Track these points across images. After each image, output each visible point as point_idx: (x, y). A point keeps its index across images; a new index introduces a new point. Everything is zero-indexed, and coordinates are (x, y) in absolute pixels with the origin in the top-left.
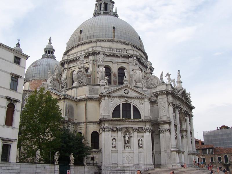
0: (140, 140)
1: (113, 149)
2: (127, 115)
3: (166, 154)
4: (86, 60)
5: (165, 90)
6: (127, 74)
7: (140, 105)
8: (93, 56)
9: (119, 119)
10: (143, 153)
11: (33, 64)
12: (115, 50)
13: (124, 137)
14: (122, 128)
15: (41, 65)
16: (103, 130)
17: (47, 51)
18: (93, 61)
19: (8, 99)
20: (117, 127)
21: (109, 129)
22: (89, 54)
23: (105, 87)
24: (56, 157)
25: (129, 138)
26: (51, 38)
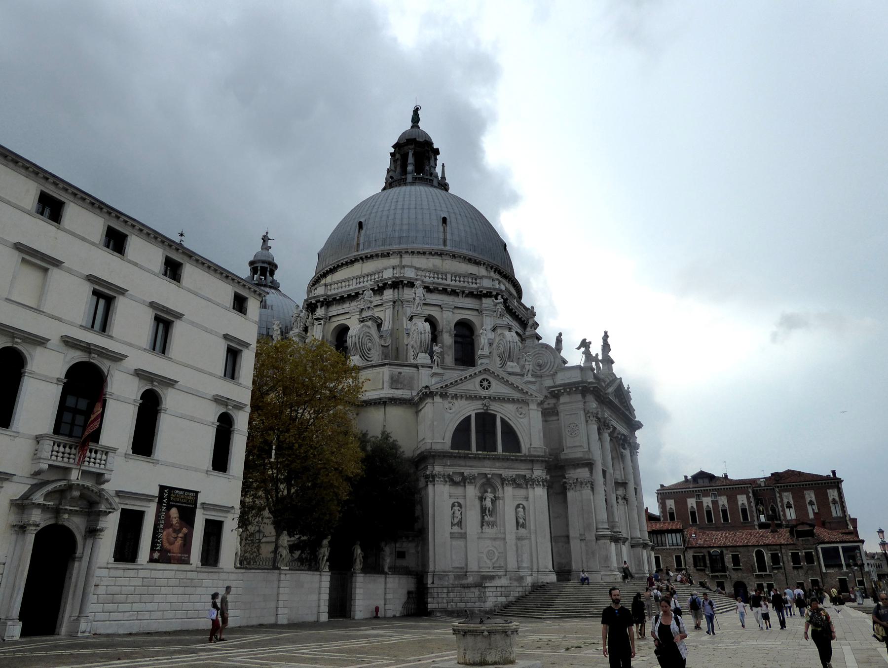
0: (520, 507)
3: (583, 544)
4: (376, 300)
5: (578, 383)
8: (394, 290)
9: (468, 452)
10: (526, 542)
12: (449, 276)
14: (476, 475)
16: (431, 482)
17: (259, 268)
18: (394, 302)
19: (218, 400)
20: (463, 473)
21: (444, 479)
23: (434, 371)
24: (325, 552)
25: (492, 503)
26: (267, 233)
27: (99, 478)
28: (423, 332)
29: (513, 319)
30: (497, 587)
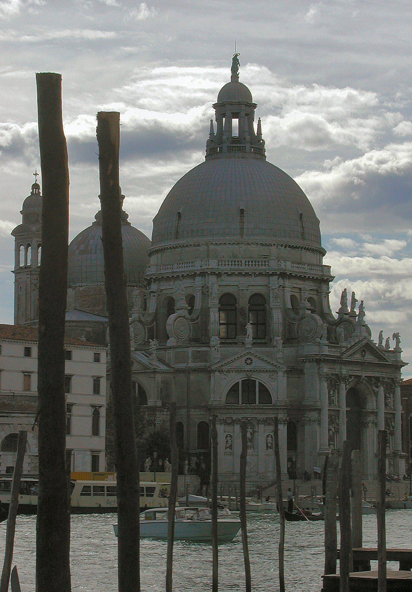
1: (225, 451)
7: (271, 383)
8: (202, 277)
12: (243, 262)
19: (93, 406)
20: (232, 418)
22: (196, 273)
28: (214, 323)
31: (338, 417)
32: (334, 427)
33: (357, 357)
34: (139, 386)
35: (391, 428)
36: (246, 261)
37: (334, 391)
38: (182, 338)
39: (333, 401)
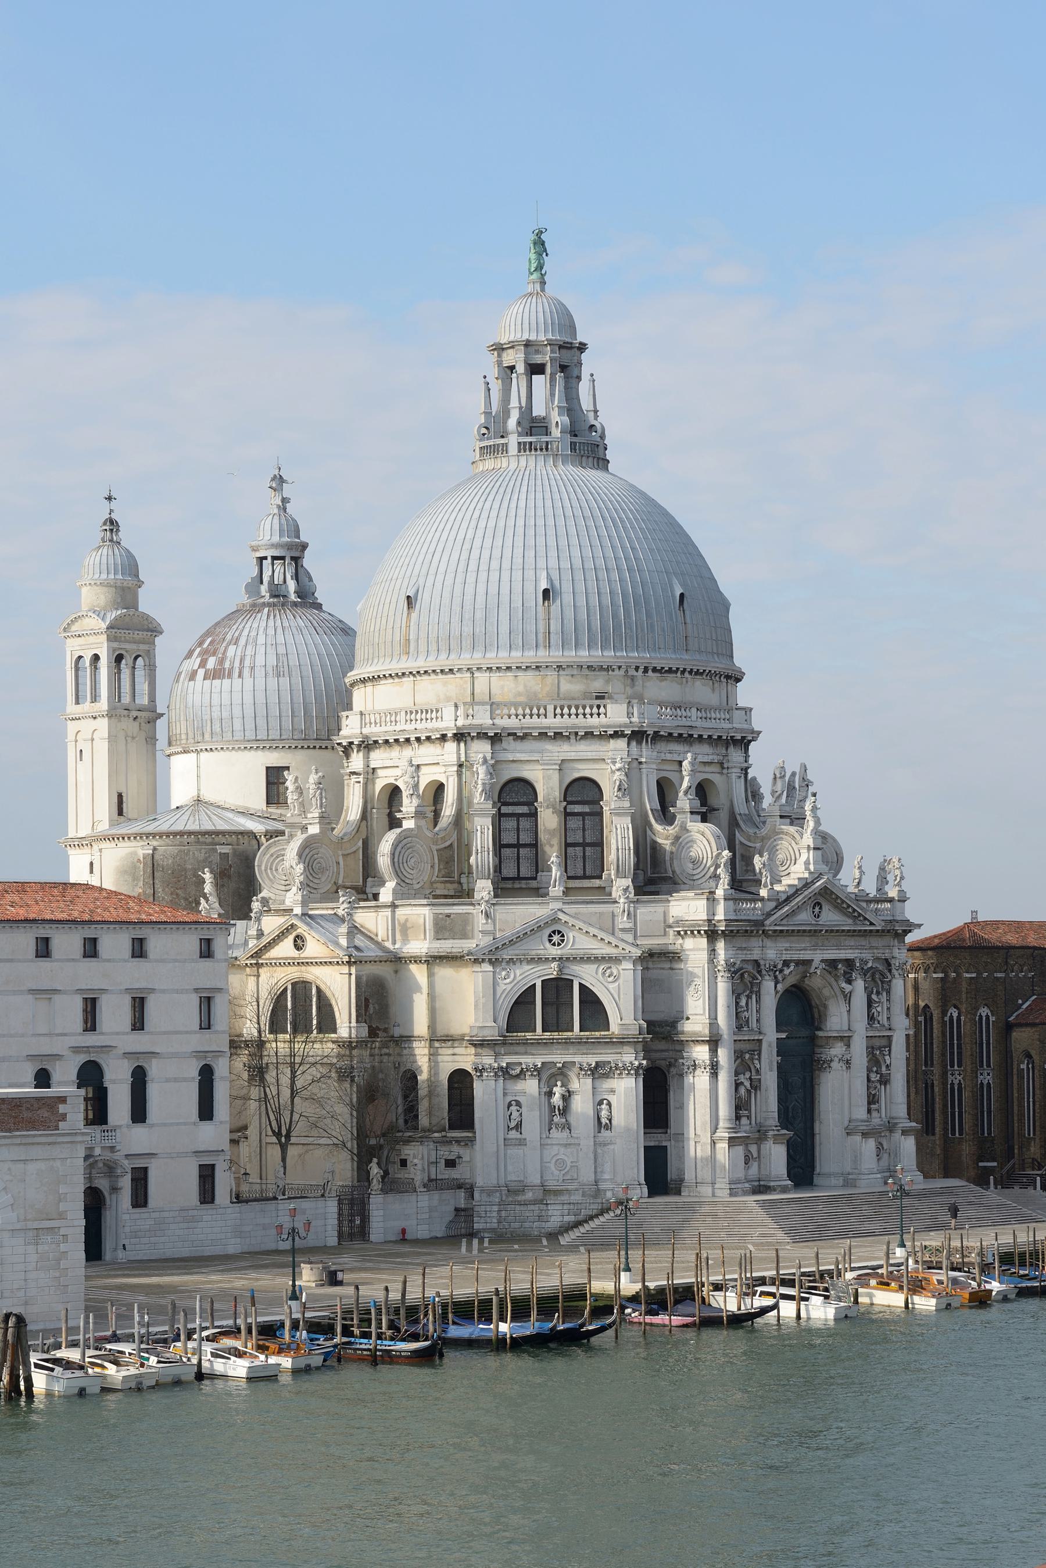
1: (509, 1136)
2: (556, 1021)
6: (558, 874)
8: (459, 744)
10: (611, 1147)
11: (200, 644)
12: (550, 708)
13: (550, 1094)
15: (246, 672)
18: (460, 766)
19: (198, 1054)
20: (521, 1064)
21: (496, 1073)
27: (112, 1149)
29: (691, 745)
30: (563, 1204)
31: (759, 1055)
32: (750, 1079)
33: (805, 917)
34: (319, 990)
35: (884, 1068)
36: (555, 709)
37: (749, 997)
38: (415, 882)
39: (747, 1021)
